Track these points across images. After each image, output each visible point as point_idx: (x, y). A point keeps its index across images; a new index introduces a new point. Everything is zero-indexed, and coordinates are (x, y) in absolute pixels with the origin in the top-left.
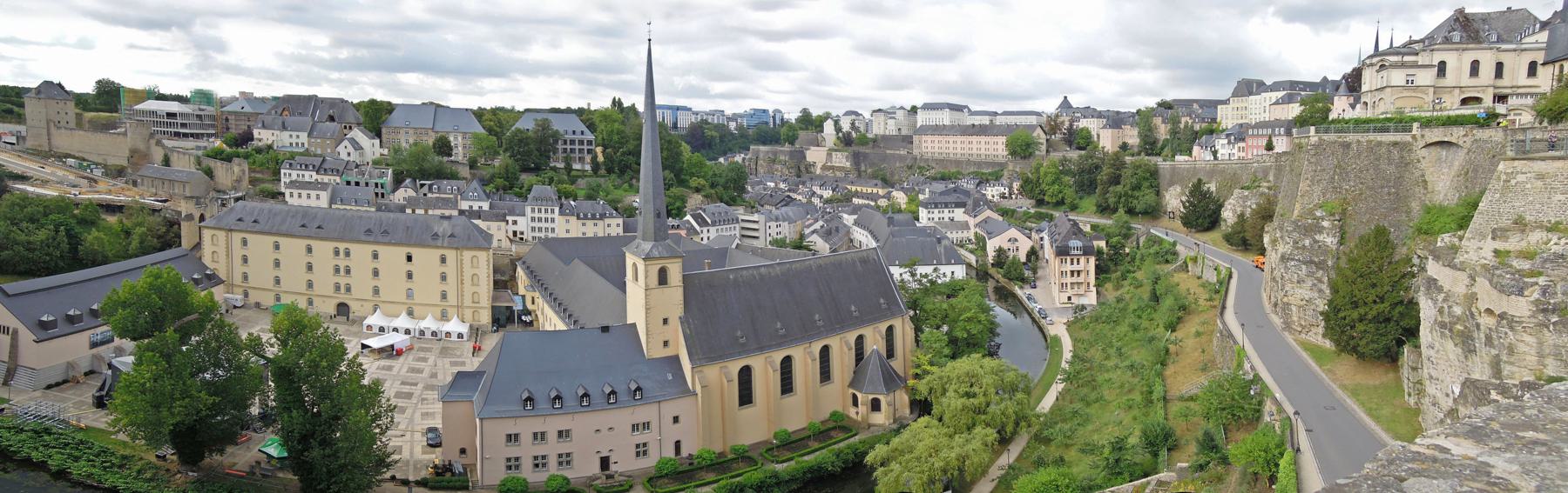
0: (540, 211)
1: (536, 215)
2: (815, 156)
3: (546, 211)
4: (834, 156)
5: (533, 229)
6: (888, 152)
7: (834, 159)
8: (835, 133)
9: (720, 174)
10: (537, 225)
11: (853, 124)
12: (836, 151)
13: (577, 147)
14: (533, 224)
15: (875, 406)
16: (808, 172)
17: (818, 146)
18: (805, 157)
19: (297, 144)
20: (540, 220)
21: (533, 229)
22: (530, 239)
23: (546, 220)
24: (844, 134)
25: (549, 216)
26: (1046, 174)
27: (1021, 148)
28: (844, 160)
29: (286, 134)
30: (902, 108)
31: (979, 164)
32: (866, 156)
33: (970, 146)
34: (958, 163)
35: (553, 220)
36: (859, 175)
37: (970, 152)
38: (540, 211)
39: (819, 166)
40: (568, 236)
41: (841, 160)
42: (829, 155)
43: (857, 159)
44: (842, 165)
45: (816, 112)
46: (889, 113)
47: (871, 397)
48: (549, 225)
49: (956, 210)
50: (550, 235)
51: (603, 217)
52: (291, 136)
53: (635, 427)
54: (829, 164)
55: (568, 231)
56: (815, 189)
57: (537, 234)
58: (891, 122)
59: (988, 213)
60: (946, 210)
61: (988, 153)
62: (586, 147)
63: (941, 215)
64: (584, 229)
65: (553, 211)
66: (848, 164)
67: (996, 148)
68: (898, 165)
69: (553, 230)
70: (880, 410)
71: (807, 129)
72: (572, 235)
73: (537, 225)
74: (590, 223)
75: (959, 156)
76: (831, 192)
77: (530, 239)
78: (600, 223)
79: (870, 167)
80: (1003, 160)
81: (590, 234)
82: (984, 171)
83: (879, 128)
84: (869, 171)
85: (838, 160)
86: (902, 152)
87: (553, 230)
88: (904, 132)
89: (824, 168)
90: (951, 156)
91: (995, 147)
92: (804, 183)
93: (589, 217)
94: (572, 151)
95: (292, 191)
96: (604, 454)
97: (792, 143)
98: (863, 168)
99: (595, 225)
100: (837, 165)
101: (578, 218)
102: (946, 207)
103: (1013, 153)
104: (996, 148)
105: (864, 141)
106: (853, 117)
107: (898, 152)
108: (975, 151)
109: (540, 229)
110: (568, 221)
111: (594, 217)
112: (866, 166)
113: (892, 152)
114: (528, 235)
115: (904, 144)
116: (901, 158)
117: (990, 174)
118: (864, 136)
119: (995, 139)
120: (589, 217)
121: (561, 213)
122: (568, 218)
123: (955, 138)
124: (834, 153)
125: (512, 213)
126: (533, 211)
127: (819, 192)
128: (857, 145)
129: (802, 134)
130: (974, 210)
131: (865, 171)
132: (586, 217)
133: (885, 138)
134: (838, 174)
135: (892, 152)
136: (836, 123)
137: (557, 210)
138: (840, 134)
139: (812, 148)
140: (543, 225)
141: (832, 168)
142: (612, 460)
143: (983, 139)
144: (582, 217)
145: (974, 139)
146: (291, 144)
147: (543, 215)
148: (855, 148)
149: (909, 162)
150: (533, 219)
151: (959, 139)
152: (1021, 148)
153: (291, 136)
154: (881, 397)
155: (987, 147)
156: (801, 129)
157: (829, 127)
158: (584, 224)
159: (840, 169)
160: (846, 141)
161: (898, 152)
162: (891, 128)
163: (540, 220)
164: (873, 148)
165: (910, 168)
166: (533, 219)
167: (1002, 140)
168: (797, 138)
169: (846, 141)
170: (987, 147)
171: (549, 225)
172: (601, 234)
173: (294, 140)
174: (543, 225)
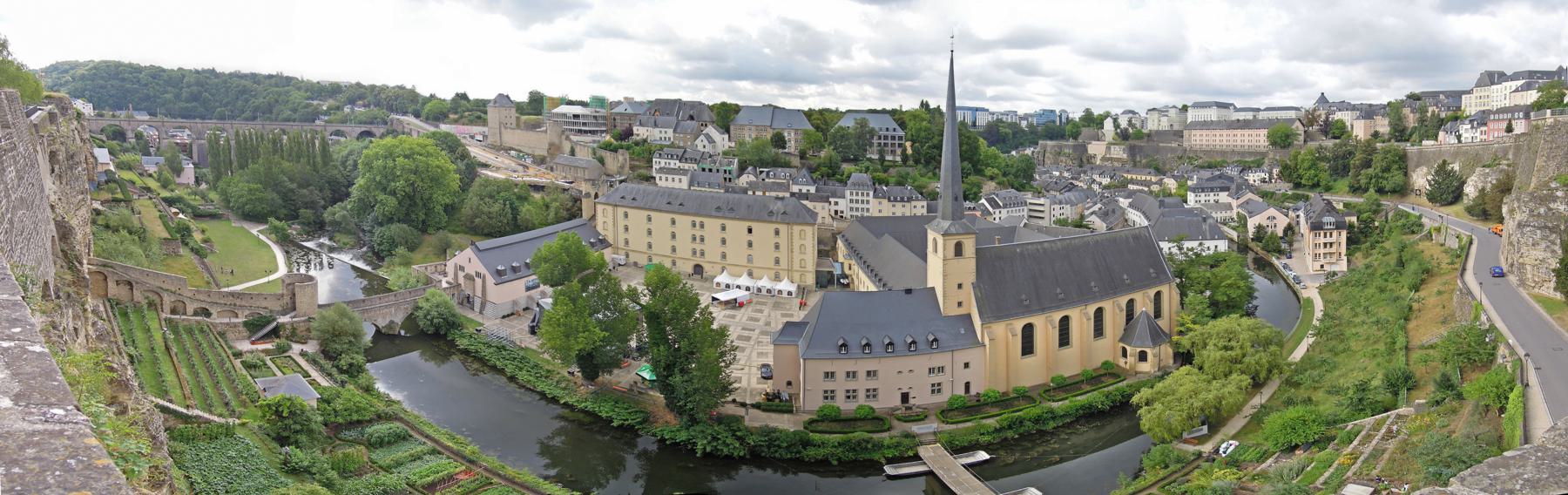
0: (857, 194)
1: (854, 197)
2: (1096, 149)
3: (863, 194)
4: (1112, 149)
5: (851, 209)
6: (1161, 145)
8: (1113, 129)
9: (1012, 165)
10: (854, 205)
11: (1130, 121)
12: (1114, 144)
13: (890, 142)
14: (852, 205)
15: (1143, 357)
16: (1089, 162)
17: (1098, 140)
18: (1087, 150)
19: (665, 138)
20: (857, 201)
21: (851, 209)
22: (849, 217)
23: (863, 202)
24: (1122, 132)
25: (865, 198)
28: (1121, 152)
29: (657, 130)
30: (1174, 107)
32: (1141, 148)
35: (868, 202)
36: (1135, 165)
38: (857, 194)
39: (1099, 157)
40: (881, 215)
41: (1119, 152)
42: (1108, 148)
43: (1132, 151)
44: (1119, 157)
46: (1162, 111)
47: (1139, 350)
48: (865, 206)
50: (866, 214)
51: (910, 200)
52: (661, 132)
53: (931, 370)
54: (1108, 156)
55: (880, 211)
56: (1095, 177)
57: (855, 213)
58: (1164, 119)
62: (897, 142)
64: (893, 210)
65: (868, 195)
66: (1125, 156)
69: (868, 210)
70: (1146, 360)
71: (1089, 126)
72: (884, 214)
73: (854, 205)
74: (899, 205)
76: (1109, 180)
77: (849, 217)
78: (907, 205)
79: (1145, 158)
81: (899, 214)
83: (1152, 125)
84: (1144, 161)
87: (868, 210)
88: (1176, 127)
89: (1104, 159)
92: (1085, 173)
93: (899, 199)
94: (886, 144)
95: (674, 176)
96: (905, 391)
97: (1075, 138)
98: (1138, 159)
99: (904, 206)
101: (889, 200)
105: (1139, 136)
106: (1131, 115)
109: (857, 209)
110: (880, 203)
111: (902, 200)
112: (1141, 157)
113: (1165, 145)
114: (847, 214)
115: (1175, 138)
118: (1140, 131)
120: (899, 199)
121: (875, 196)
122: (881, 200)
124: (1112, 147)
125: (834, 196)
126: (852, 194)
127: (1098, 179)
128: (1132, 139)
129: (1085, 131)
131: (1140, 162)
132: (895, 200)
133: (1158, 133)
134: (1116, 164)
135: (1165, 145)
136: (1115, 120)
137: (871, 193)
138: (1119, 130)
139: (1094, 142)
140: (860, 206)
141: (1111, 159)
142: (911, 396)
144: (893, 200)
146: (661, 138)
147: (860, 198)
148: (1131, 142)
150: (851, 201)
153: (661, 132)
154: (1148, 350)
156: (1084, 126)
157: (1108, 125)
158: (894, 206)
159: (1118, 160)
160: (1123, 136)
162: (1164, 124)
163: (857, 201)
164: (1148, 141)
166: (851, 201)
168: (1080, 134)
169: (1123, 136)
171: (865, 206)
173: (663, 135)
174: (860, 206)
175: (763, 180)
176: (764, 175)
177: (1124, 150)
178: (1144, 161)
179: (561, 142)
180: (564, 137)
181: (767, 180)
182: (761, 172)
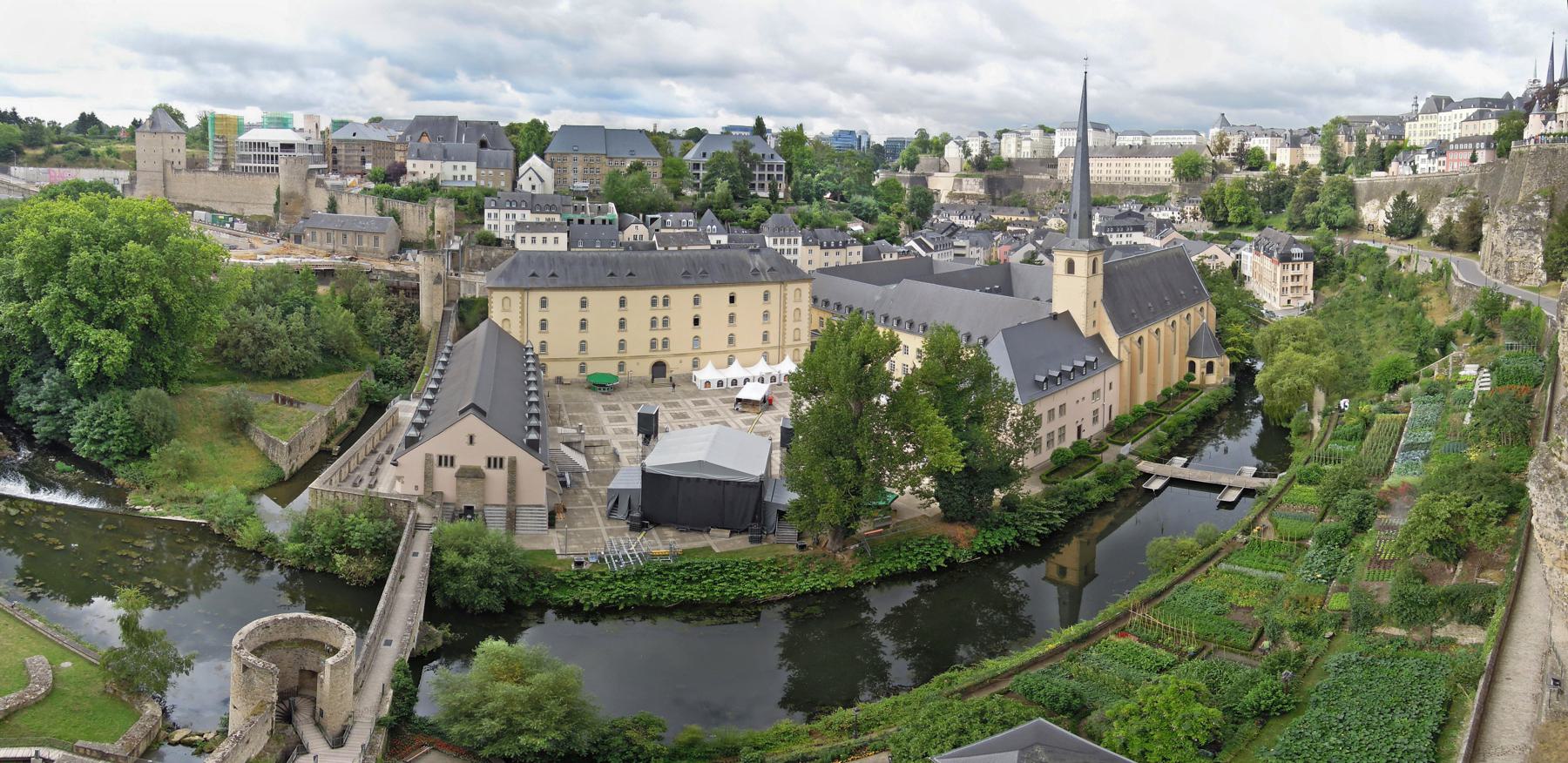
2: (941, 184)
4: (964, 182)
7: (964, 186)
12: (967, 176)
17: (940, 171)
18: (926, 185)
19: (463, 177)
26: (1231, 195)
27: (1190, 170)
28: (977, 187)
29: (449, 165)
31: (1138, 188)
33: (1128, 169)
34: (1112, 187)
37: (1127, 175)
43: (991, 184)
45: (934, 133)
49: (1134, 234)
52: (455, 167)
54: (958, 192)
59: (1175, 235)
60: (1124, 234)
61: (1147, 176)
62: (766, 173)
63: (1119, 240)
66: (982, 192)
67: (1161, 170)
68: (1038, 191)
75: (1113, 180)
76: (973, 221)
80: (1167, 183)
82: (1144, 195)
85: (969, 187)
86: (1043, 177)
89: (951, 195)
90: (1104, 180)
91: (1157, 169)
98: (997, 196)
100: (968, 192)
102: (1125, 231)
103: (1179, 175)
104: (1161, 170)
107: (1038, 177)
108: (1132, 174)
113: (1031, 177)
115: (1043, 168)
116: (1043, 184)
117: (1151, 198)
119: (1157, 161)
123: (1109, 161)
124: (964, 179)
126: (775, 242)
130: (1158, 232)
133: (1020, 161)
134: (970, 202)
135: (1031, 177)
139: (936, 174)
141: (962, 196)
143: (1143, 161)
145: (1133, 161)
146: (455, 177)
149: (1052, 188)
151: (1114, 161)
152: (1190, 170)
153: (455, 167)
155: (1148, 169)
159: (973, 197)
161: (1038, 177)
165: (1054, 194)
167: (1169, 161)
170: (1148, 169)
172: (842, 263)
173: (459, 173)
175: (657, 230)
176: (657, 224)
177: (980, 183)
178: (1004, 198)
179: (306, 190)
180: (312, 182)
181: (663, 231)
182: (653, 220)
